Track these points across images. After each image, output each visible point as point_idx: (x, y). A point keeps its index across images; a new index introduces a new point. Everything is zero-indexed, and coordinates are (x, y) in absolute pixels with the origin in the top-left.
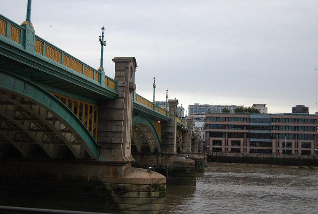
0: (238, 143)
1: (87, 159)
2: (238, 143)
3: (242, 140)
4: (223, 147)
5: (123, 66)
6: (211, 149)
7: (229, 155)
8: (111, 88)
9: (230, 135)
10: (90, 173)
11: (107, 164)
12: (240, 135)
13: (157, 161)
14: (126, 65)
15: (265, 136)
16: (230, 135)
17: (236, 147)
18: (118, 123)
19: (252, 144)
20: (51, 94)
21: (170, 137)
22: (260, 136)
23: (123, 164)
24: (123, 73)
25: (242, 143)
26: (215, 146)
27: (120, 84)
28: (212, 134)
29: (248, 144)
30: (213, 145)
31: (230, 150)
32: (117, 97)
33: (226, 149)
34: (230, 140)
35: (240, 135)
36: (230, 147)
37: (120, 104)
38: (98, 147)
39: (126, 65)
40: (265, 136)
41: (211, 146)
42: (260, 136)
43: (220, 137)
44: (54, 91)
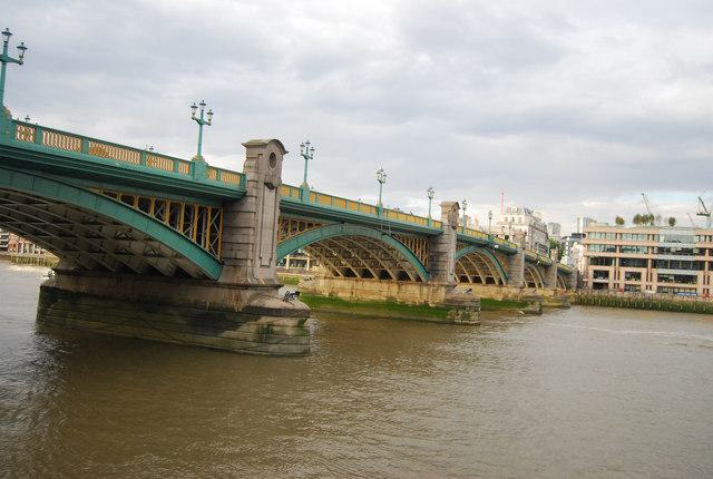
0: (638, 276)
1: (203, 280)
2: (638, 276)
3: (643, 271)
4: (611, 281)
5: (256, 152)
6: (591, 284)
7: (619, 294)
8: (232, 184)
9: (624, 262)
10: (211, 297)
11: (231, 286)
12: (643, 263)
13: (421, 294)
14: (268, 153)
15: (686, 265)
16: (624, 262)
17: (633, 282)
18: (245, 231)
19: (661, 278)
20: (97, 191)
21: (441, 259)
22: (674, 264)
23: (246, 287)
24: (253, 163)
25: (643, 277)
26: (597, 280)
27: (248, 178)
28: (596, 261)
29: (655, 277)
30: (628, 279)
31: (622, 286)
32: (244, 195)
33: (616, 286)
34: (623, 270)
35: (643, 263)
36: (622, 282)
37: (250, 204)
38: (221, 264)
39: (268, 153)
40: (686, 265)
41: (591, 281)
42: (674, 264)
43: (606, 265)
44: (104, 185)
